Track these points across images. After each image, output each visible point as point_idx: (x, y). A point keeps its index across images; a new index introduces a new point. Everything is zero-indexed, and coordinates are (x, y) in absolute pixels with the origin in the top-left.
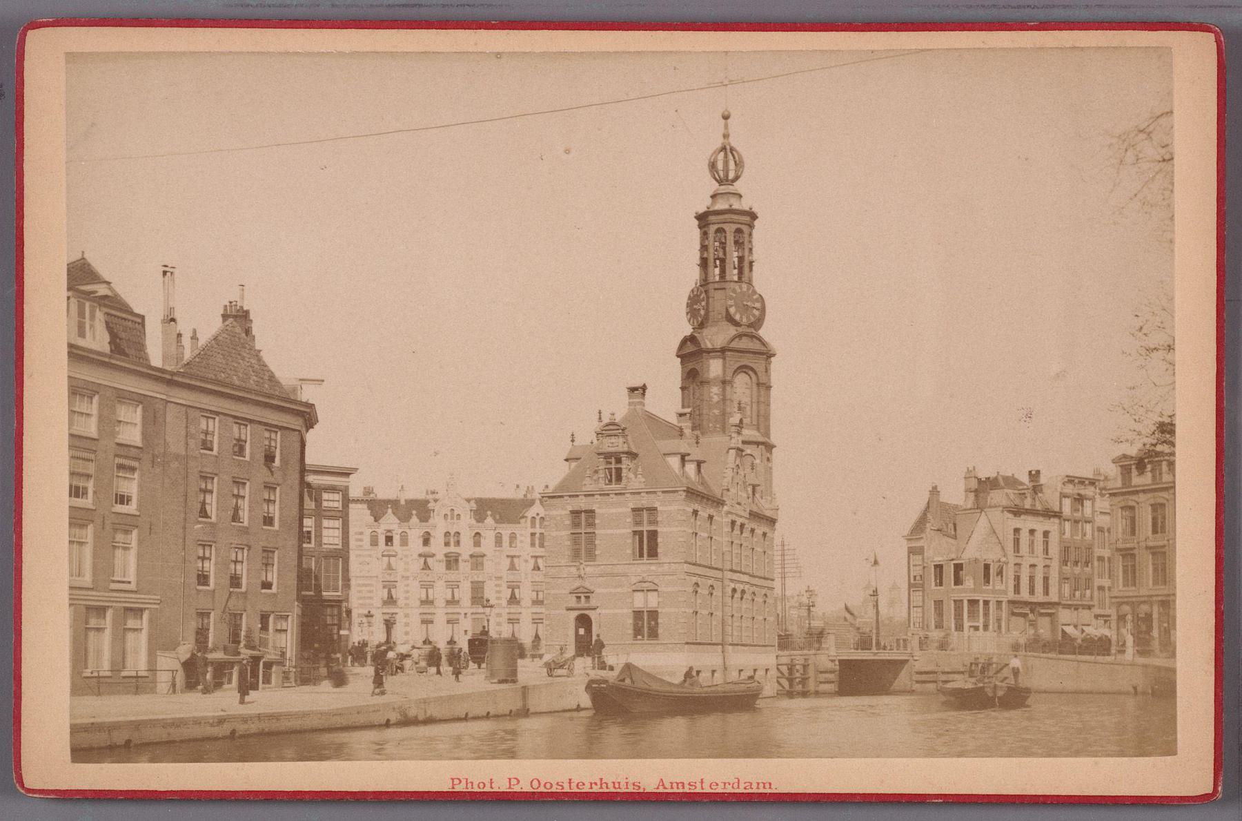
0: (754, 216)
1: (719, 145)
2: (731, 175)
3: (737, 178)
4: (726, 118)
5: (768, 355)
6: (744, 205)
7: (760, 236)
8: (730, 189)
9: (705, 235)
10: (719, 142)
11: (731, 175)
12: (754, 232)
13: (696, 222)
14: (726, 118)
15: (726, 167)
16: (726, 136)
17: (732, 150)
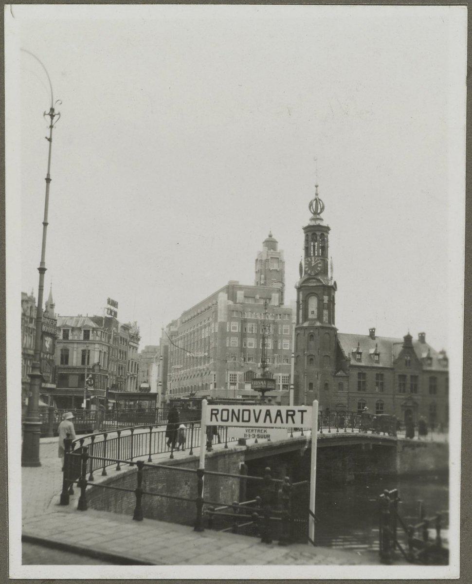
0: (327, 229)
1: (314, 198)
2: (319, 211)
3: (321, 212)
4: (317, 186)
5: (334, 288)
6: (324, 224)
7: (331, 237)
8: (318, 216)
9: (307, 236)
10: (313, 197)
11: (319, 211)
12: (329, 236)
13: (303, 231)
14: (317, 186)
15: (317, 207)
16: (317, 194)
17: (319, 200)
